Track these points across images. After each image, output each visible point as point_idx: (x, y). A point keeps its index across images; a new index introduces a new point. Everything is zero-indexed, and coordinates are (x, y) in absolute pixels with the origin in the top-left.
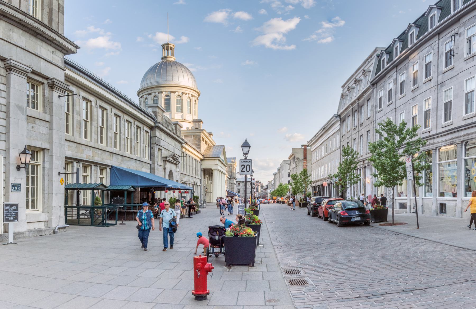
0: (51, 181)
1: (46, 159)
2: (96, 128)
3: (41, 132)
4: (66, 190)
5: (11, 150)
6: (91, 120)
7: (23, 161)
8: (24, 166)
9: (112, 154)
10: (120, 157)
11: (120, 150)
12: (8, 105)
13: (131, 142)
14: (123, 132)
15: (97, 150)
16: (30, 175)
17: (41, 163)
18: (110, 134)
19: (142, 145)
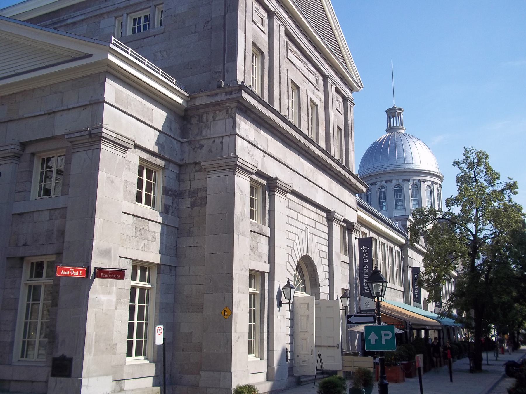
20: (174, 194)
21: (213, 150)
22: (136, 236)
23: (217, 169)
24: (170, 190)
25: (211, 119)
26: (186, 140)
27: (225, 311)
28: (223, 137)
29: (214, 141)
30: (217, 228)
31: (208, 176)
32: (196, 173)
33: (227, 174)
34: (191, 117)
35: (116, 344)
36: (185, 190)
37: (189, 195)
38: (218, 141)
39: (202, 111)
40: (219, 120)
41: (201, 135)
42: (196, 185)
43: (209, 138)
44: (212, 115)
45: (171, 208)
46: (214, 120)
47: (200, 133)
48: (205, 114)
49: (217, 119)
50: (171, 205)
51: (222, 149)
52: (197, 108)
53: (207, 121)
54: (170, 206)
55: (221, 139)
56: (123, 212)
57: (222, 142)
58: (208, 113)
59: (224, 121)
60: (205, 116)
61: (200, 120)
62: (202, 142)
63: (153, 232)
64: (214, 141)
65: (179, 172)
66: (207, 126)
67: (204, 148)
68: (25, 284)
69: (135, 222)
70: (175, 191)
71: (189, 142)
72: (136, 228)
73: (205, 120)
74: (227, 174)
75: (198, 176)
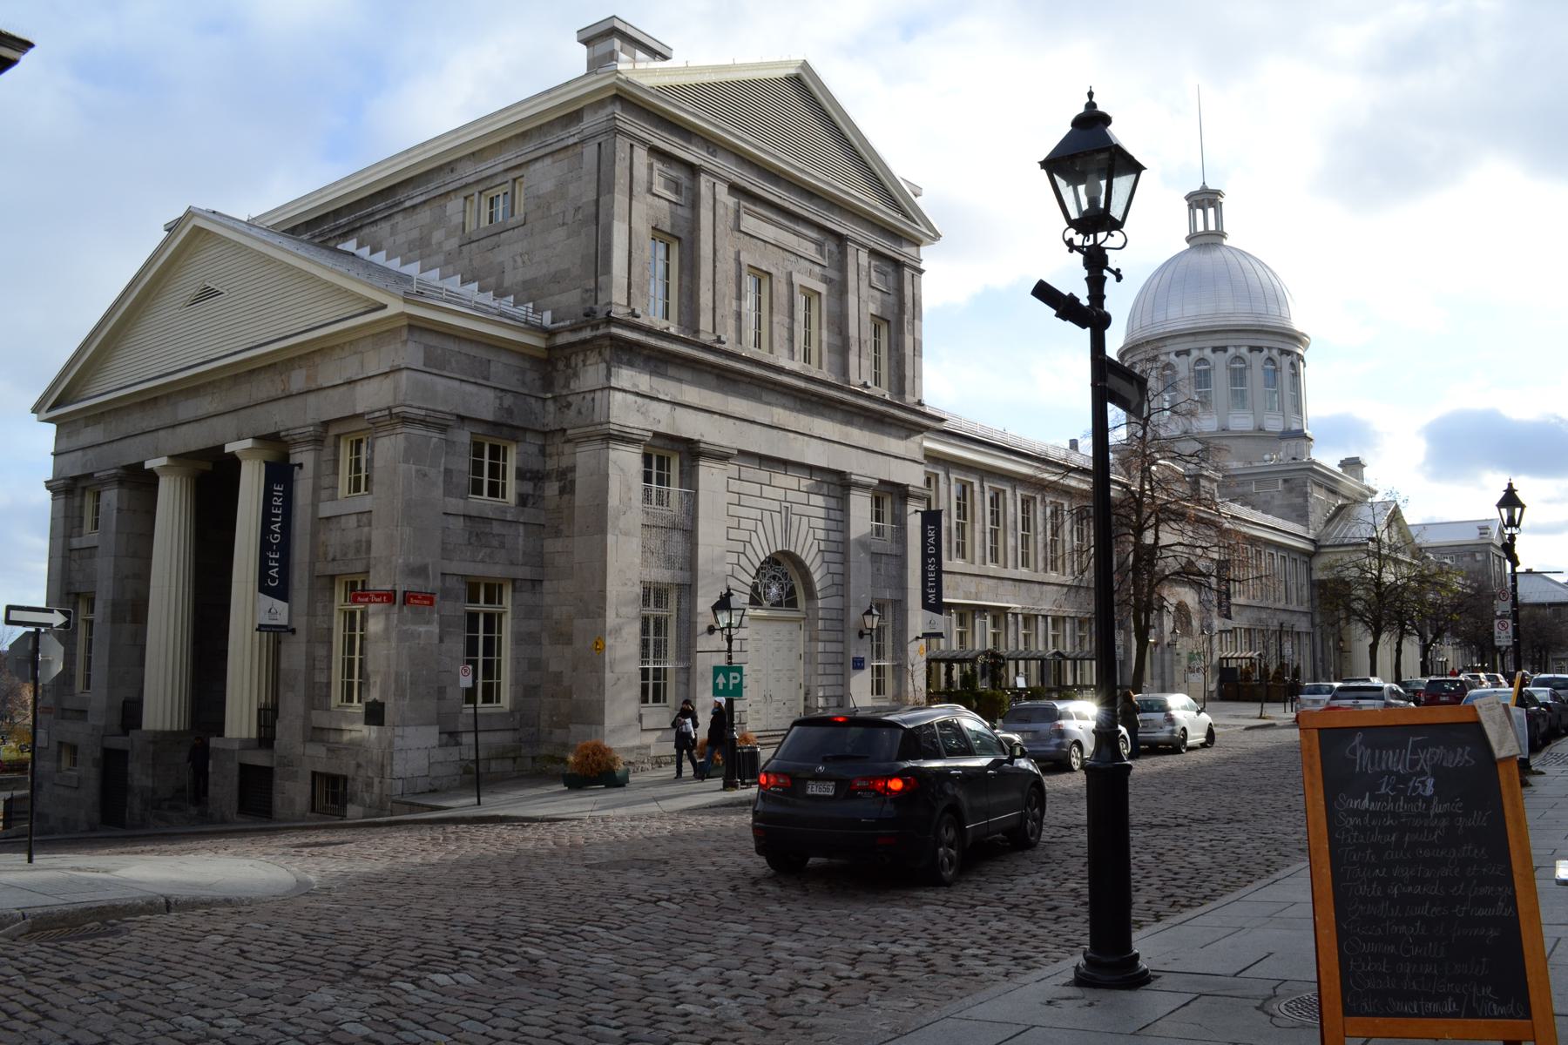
4: (929, 661)
5: (852, 610)
7: (869, 626)
9: (1017, 583)
10: (1037, 587)
16: (875, 643)
18: (1011, 542)
21: (583, 410)
22: (470, 544)
24: (531, 471)
25: (580, 364)
27: (597, 643)
31: (578, 450)
34: (557, 359)
37: (557, 477)
41: (568, 387)
42: (565, 462)
44: (581, 357)
45: (530, 498)
46: (584, 365)
47: (567, 385)
48: (574, 356)
49: (588, 362)
50: (531, 492)
53: (576, 365)
56: (445, 514)
61: (568, 366)
62: (570, 399)
63: (499, 535)
64: (584, 398)
66: (576, 375)
67: (573, 407)
69: (469, 524)
71: (554, 398)
72: (470, 533)
73: (573, 365)
75: (568, 448)
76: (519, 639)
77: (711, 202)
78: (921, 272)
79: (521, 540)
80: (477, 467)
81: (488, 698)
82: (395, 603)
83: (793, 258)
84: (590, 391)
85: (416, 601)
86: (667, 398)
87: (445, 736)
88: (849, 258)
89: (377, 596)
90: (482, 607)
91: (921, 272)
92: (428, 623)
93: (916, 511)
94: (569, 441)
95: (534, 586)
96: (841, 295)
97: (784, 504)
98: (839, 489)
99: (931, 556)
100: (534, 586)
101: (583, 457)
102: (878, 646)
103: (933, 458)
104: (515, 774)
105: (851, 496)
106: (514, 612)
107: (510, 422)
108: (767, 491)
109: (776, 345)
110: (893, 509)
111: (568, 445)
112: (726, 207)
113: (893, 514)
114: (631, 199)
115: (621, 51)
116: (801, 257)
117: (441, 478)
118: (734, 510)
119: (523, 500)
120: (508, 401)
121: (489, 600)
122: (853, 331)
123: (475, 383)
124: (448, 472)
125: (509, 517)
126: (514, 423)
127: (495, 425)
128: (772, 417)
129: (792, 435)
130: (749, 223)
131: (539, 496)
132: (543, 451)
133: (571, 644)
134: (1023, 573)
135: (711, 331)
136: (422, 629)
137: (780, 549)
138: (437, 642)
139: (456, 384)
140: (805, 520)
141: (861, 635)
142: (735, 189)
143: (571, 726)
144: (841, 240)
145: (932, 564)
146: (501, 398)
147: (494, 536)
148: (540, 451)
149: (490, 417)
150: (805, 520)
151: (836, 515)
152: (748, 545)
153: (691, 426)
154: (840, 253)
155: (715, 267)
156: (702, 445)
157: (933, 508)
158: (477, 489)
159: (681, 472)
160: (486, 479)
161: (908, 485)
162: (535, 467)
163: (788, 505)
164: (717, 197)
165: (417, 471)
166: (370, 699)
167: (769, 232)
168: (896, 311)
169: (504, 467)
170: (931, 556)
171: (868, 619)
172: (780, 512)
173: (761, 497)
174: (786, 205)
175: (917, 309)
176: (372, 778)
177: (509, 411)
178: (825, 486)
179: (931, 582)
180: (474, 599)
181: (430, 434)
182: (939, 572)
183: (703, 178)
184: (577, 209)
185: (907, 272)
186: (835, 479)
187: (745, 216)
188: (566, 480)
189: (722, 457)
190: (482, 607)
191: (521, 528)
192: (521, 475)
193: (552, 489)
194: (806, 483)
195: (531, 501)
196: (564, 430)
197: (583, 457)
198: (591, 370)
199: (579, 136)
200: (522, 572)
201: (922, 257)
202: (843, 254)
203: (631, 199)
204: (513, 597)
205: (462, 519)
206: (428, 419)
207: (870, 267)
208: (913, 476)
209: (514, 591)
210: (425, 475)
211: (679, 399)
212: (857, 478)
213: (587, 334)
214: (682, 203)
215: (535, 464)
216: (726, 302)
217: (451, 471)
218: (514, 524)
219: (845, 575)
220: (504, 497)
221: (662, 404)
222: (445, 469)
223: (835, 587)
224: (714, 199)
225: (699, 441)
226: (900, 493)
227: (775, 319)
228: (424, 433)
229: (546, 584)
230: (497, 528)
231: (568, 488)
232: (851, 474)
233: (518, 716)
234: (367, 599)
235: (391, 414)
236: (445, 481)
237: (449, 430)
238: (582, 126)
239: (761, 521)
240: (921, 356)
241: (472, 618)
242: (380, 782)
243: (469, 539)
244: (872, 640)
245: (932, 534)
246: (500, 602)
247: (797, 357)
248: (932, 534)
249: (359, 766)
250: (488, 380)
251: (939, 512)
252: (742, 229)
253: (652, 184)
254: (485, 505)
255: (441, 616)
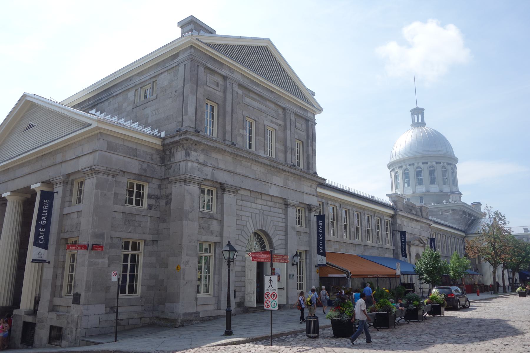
0: (311, 271)
1: (308, 257)
2: (341, 226)
3: (304, 240)
6: (337, 221)
8: (296, 263)
11: (362, 241)
12: (286, 227)
13: (372, 232)
14: (364, 225)
15: (342, 243)
16: (298, 268)
17: (305, 260)
18: (352, 229)
19: (384, 233)
20: (156, 198)
21: (176, 170)
22: (125, 225)
23: (176, 182)
26: (163, 164)
28: (180, 162)
29: (176, 164)
30: (176, 218)
31: (173, 186)
32: (168, 184)
33: (182, 184)
34: (166, 150)
35: (110, 287)
36: (163, 195)
38: (178, 164)
39: (171, 146)
40: (179, 151)
41: (170, 161)
43: (174, 163)
44: (176, 148)
46: (177, 152)
47: (169, 160)
48: (173, 148)
51: (180, 169)
52: (168, 145)
53: (174, 152)
54: (152, 205)
55: (179, 163)
57: (180, 165)
58: (174, 147)
59: (181, 152)
60: (172, 149)
61: (170, 152)
63: (139, 221)
64: (176, 164)
65: (160, 184)
66: (173, 155)
68: (69, 253)
70: (157, 196)
71: (165, 166)
73: (172, 152)
74: (182, 184)
75: (169, 186)
76: (145, 266)
77: (231, 90)
78: (316, 124)
79: (148, 223)
80: (131, 193)
81: (131, 291)
82: (88, 249)
83: (265, 115)
84: (179, 162)
85: (97, 249)
86: (211, 166)
87: (108, 309)
88: (287, 116)
89: (79, 246)
90: (130, 252)
91: (316, 124)
92: (103, 258)
93: (315, 215)
94: (170, 183)
95: (154, 243)
96: (284, 131)
97: (260, 211)
98: (283, 205)
99: (321, 233)
100: (154, 243)
101: (176, 189)
102: (300, 269)
103: (318, 195)
104: (141, 325)
105: (288, 209)
106: (144, 254)
107: (145, 174)
108: (253, 205)
109: (257, 148)
110: (305, 214)
111: (170, 184)
112: (237, 93)
113: (305, 216)
114: (197, 87)
115: (194, 30)
116: (268, 115)
117: (113, 196)
118: (239, 212)
119: (150, 207)
120: (145, 166)
121: (134, 248)
122: (289, 144)
123: (130, 158)
124: (116, 194)
125: (143, 214)
126: (147, 175)
127: (139, 175)
128: (256, 175)
129: (264, 183)
130: (247, 100)
131: (157, 206)
132: (160, 187)
133: (167, 268)
134: (358, 241)
135: (230, 140)
136: (100, 261)
137: (259, 229)
138: (107, 266)
139: (122, 157)
140: (269, 218)
141: (293, 265)
142: (240, 86)
143: (166, 304)
144: (284, 109)
145: (321, 236)
146: (141, 165)
147: (136, 222)
148: (158, 187)
149: (136, 172)
150: (269, 218)
151: (283, 216)
152: (245, 227)
153: (222, 177)
154: (283, 115)
155: (232, 115)
156: (225, 185)
157: (321, 214)
158: (131, 202)
159: (217, 196)
160: (134, 198)
161: (311, 205)
162: (156, 194)
163: (263, 211)
164: (234, 89)
165: (102, 193)
166: (75, 292)
167: (255, 104)
168: (306, 138)
169: (143, 193)
170: (321, 233)
171: (295, 258)
172: (259, 214)
173: (251, 208)
174: (262, 94)
175: (314, 138)
176: (73, 329)
177: (145, 170)
178: (278, 204)
179: (321, 243)
180: (126, 247)
181: (108, 178)
182: (324, 239)
183: (228, 81)
184: (176, 92)
185: (310, 123)
186: (282, 201)
187: (245, 97)
188: (168, 198)
189: (236, 190)
190: (130, 252)
191: (149, 218)
192: (149, 196)
193: (163, 202)
194: (270, 204)
195: (154, 207)
196: (168, 178)
197: (176, 189)
198: (179, 153)
199: (177, 62)
200: (149, 237)
201: (315, 118)
202: (285, 114)
203: (197, 87)
204: (144, 248)
205: (122, 213)
206: (107, 171)
207: (295, 121)
208: (314, 201)
209: (145, 245)
210: (105, 195)
211: (216, 166)
212: (291, 201)
213: (177, 138)
214: (219, 91)
215: (156, 192)
216: (237, 129)
217: (118, 194)
218: (146, 217)
219: (286, 240)
220: (142, 205)
221: (209, 168)
222: (115, 193)
223: (282, 245)
224: (232, 90)
225: (224, 184)
226: (310, 208)
227: (257, 138)
228: (106, 177)
229: (159, 242)
230: (138, 218)
231: (169, 203)
232: (288, 199)
233: (144, 299)
234: (74, 248)
235: (91, 169)
236: (114, 198)
237: (117, 177)
238: (179, 58)
239: (251, 217)
240: (315, 156)
241: (126, 256)
242: (76, 331)
243: (125, 222)
244: (297, 267)
245: (321, 224)
246: (139, 250)
247: (266, 153)
248: (321, 224)
249: (68, 323)
250: (136, 157)
251: (324, 216)
252: (244, 102)
253: (207, 82)
254: (133, 208)
255: (109, 255)
